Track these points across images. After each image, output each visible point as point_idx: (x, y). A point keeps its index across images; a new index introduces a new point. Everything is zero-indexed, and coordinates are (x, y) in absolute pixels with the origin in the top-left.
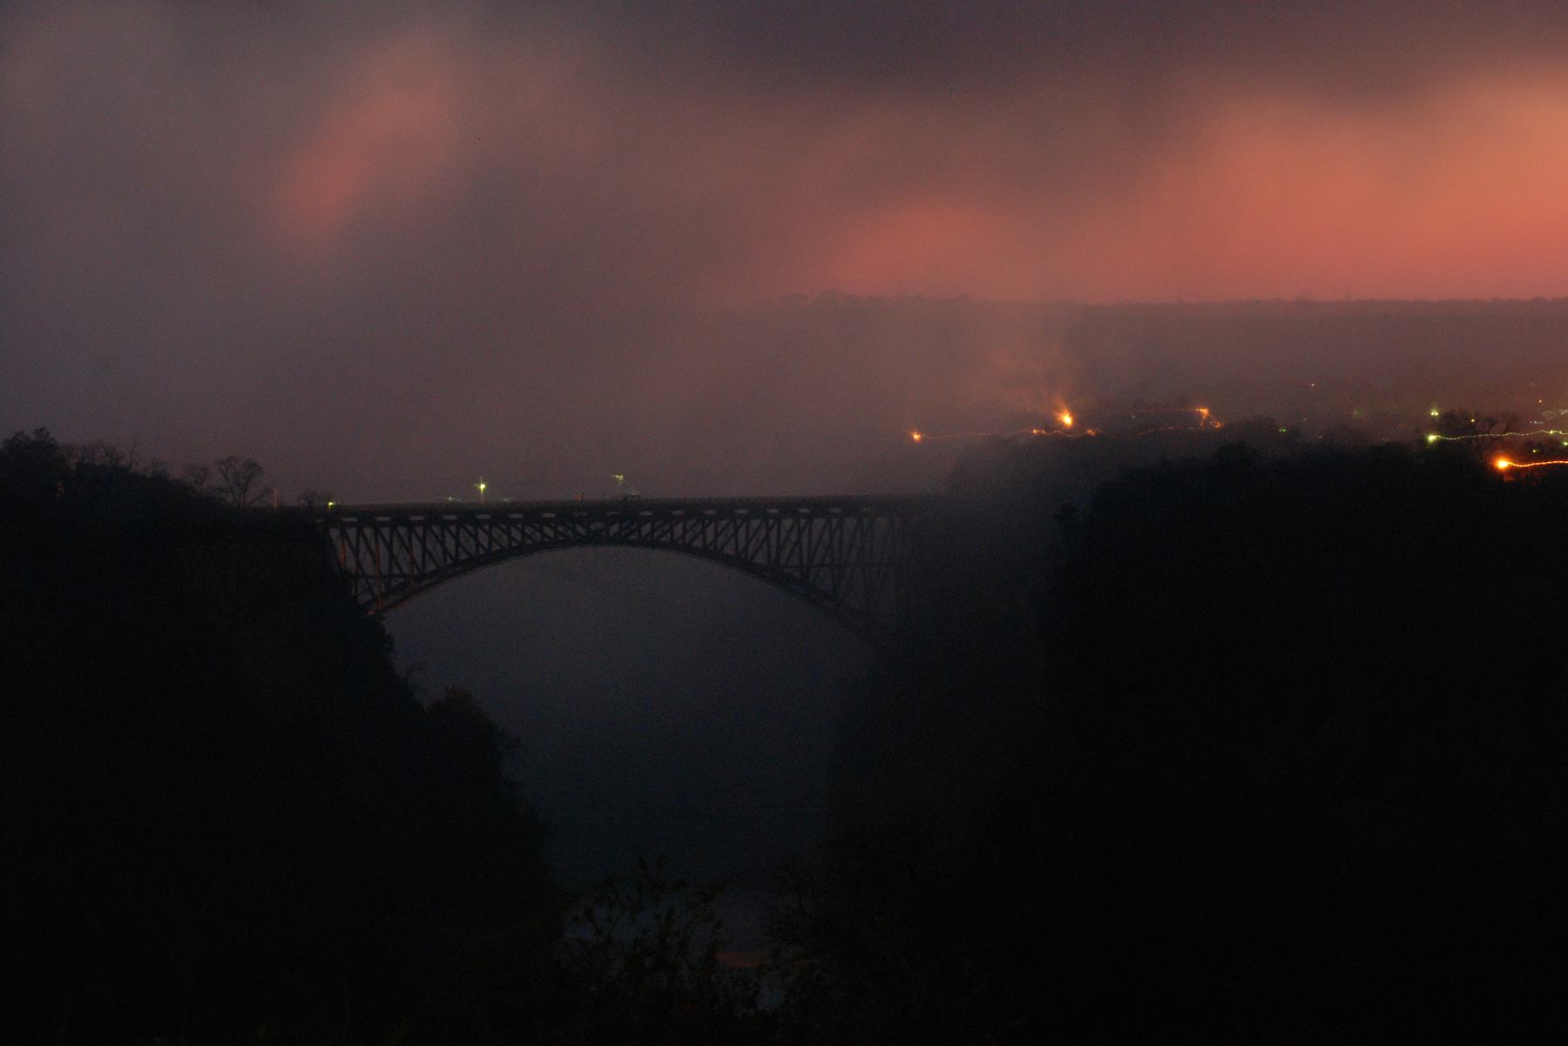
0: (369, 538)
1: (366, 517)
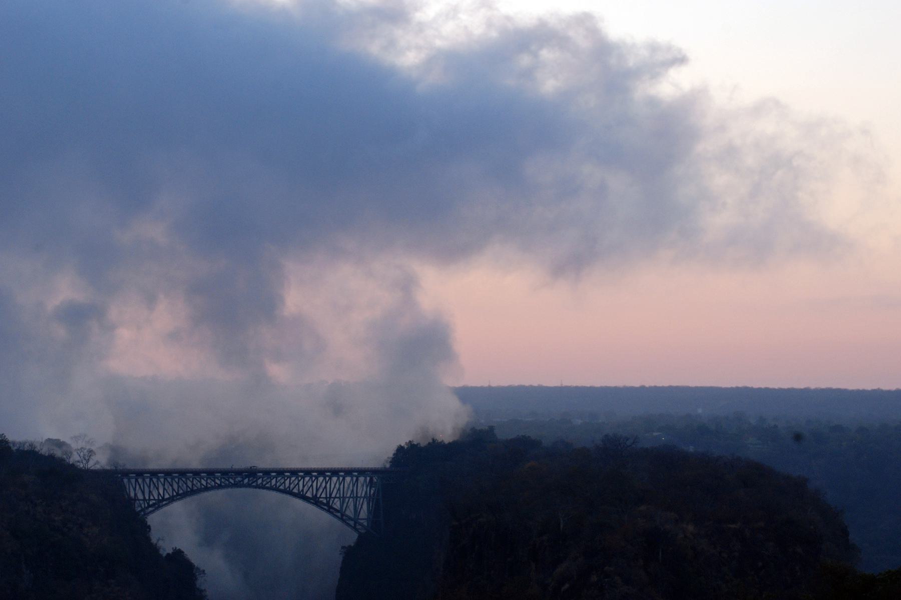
1: (140, 474)
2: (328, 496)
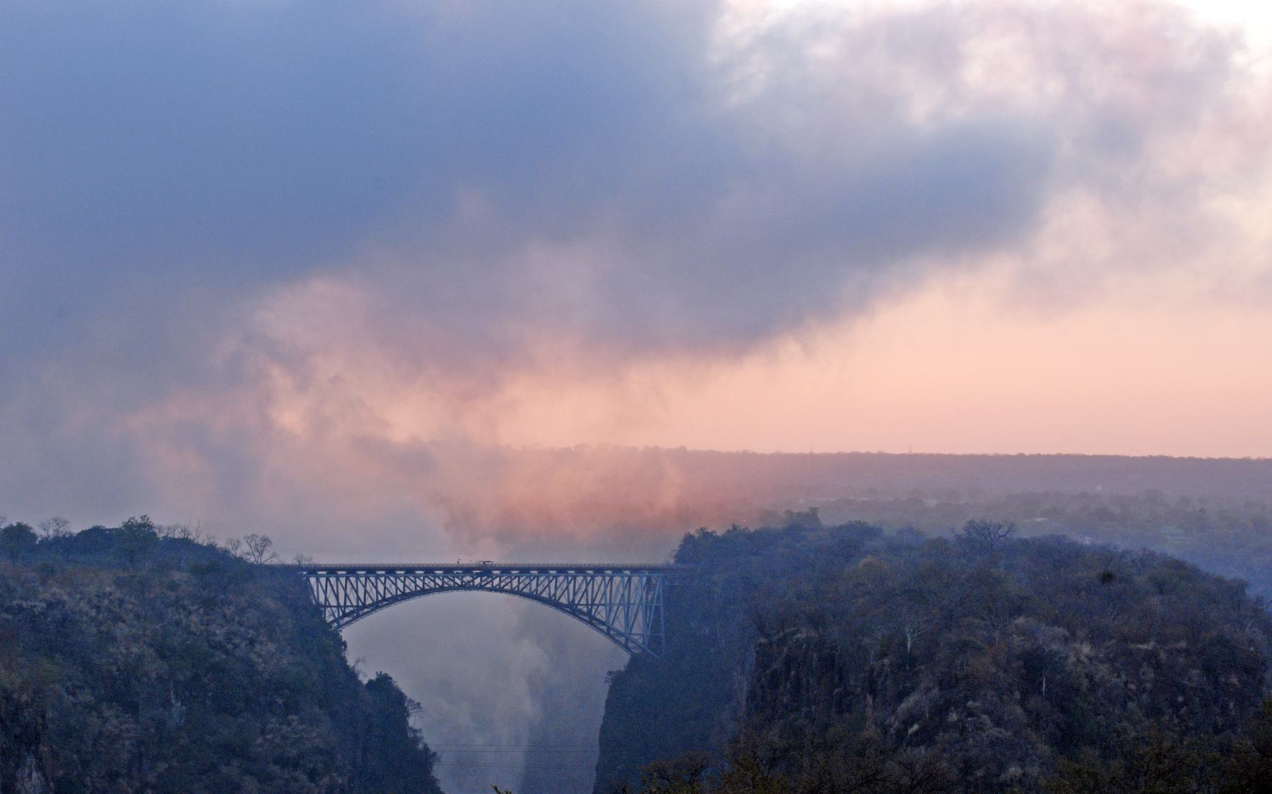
0: (332, 584)
1: (332, 571)
2: (590, 603)
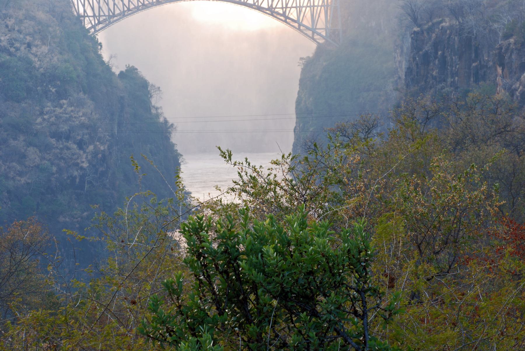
2: (284, 6)
